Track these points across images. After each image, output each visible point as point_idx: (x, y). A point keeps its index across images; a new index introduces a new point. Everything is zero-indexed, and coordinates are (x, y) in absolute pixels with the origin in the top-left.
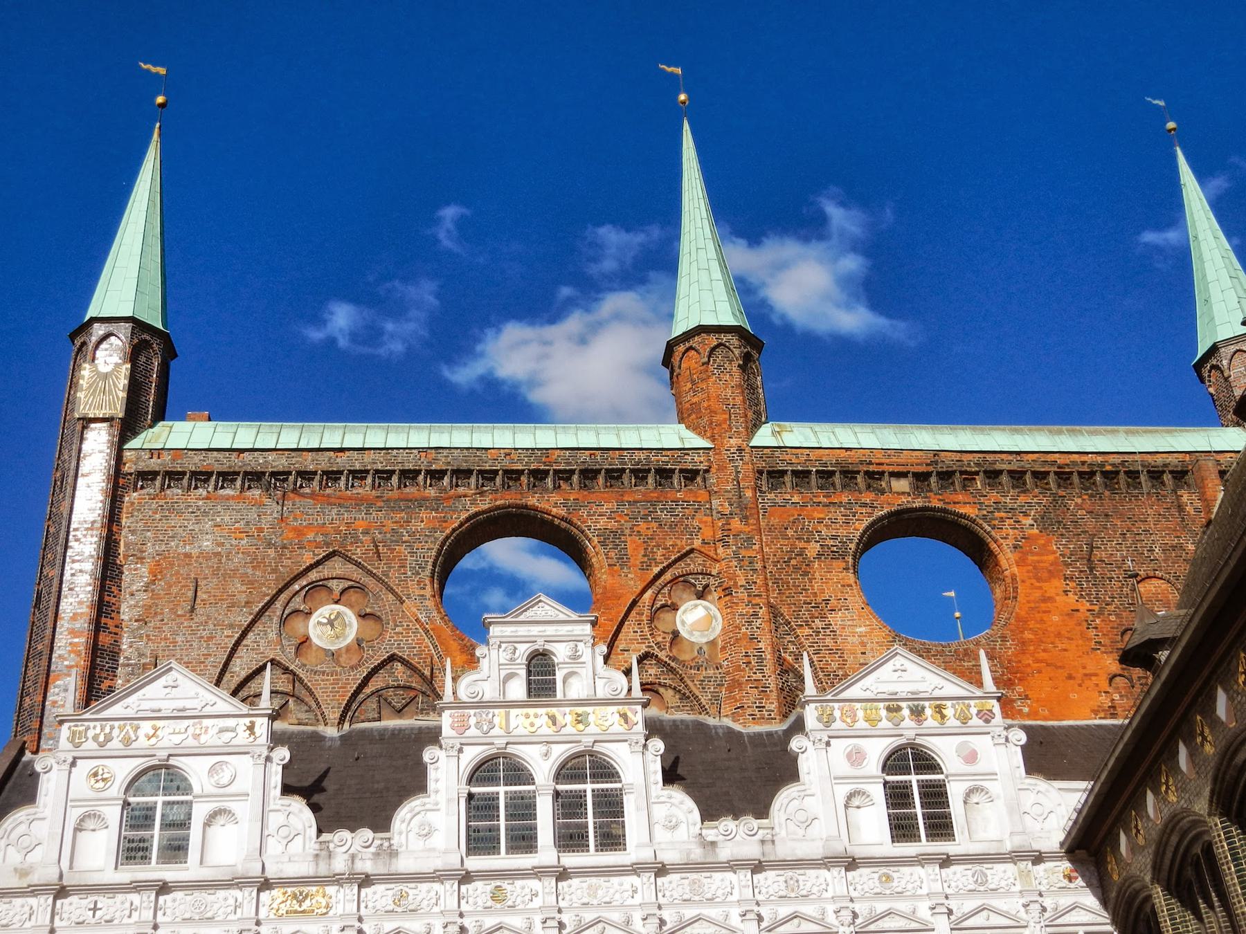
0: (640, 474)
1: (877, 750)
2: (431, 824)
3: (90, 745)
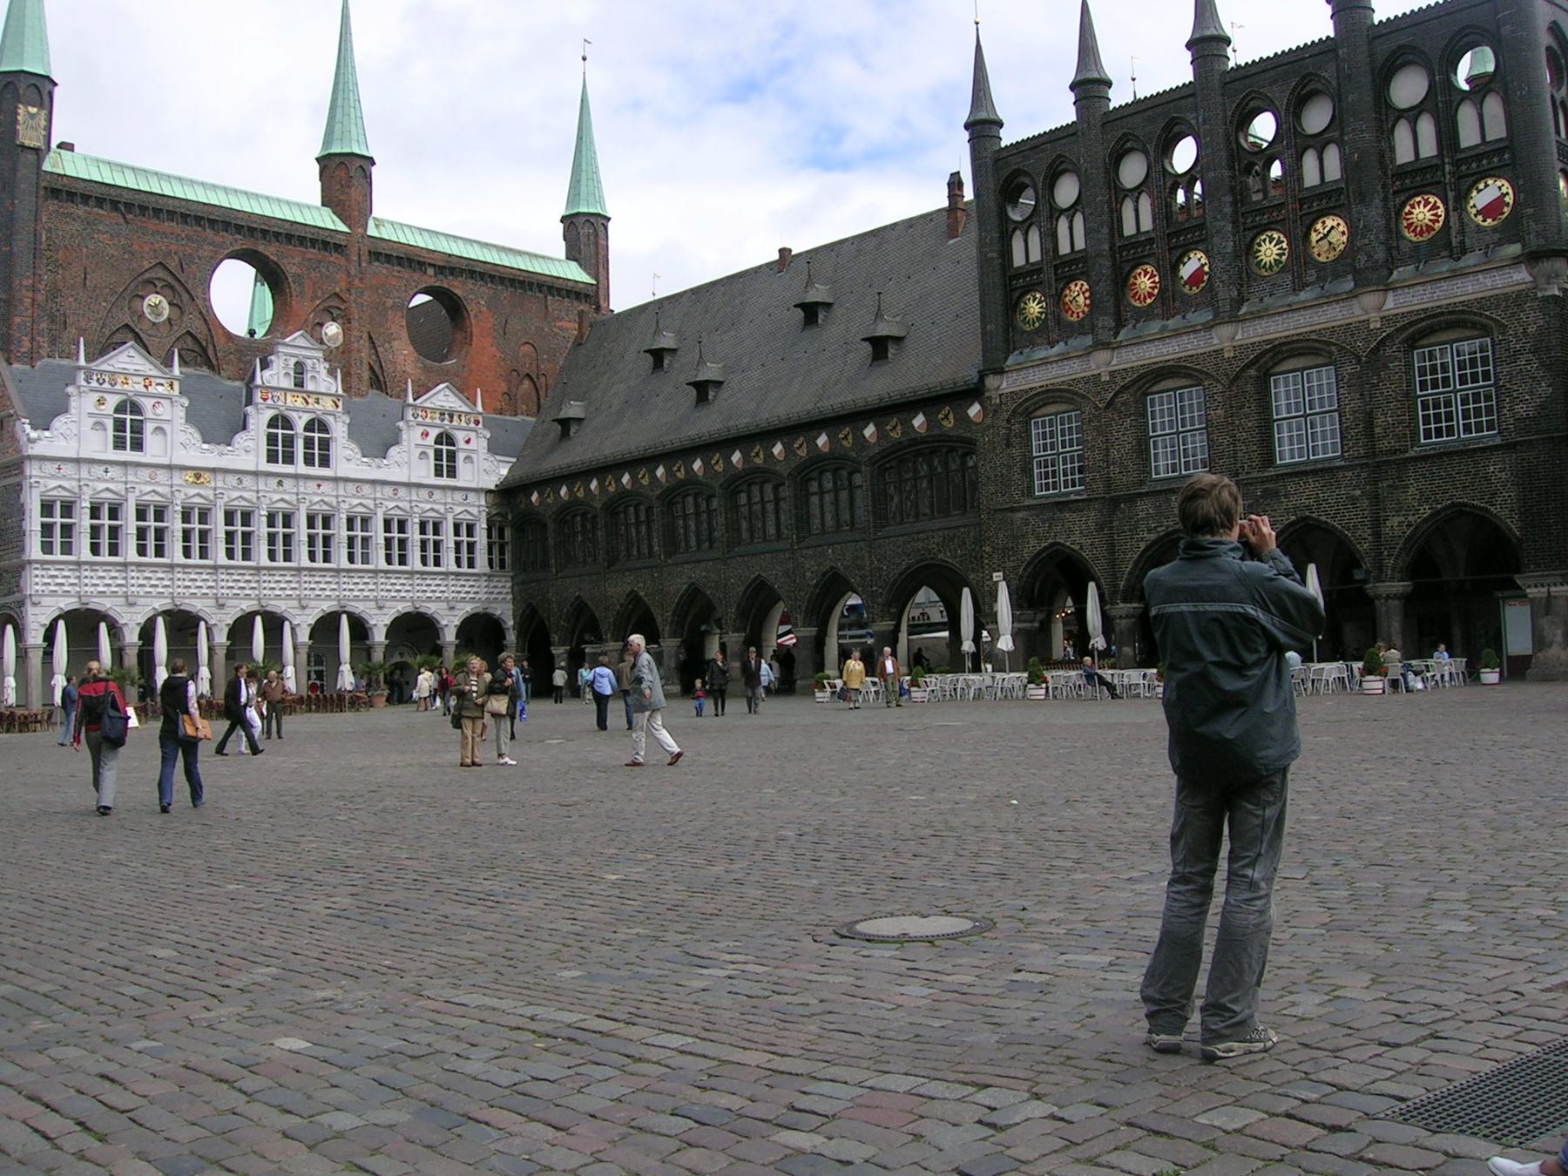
0: (314, 242)
1: (434, 433)
3: (94, 384)
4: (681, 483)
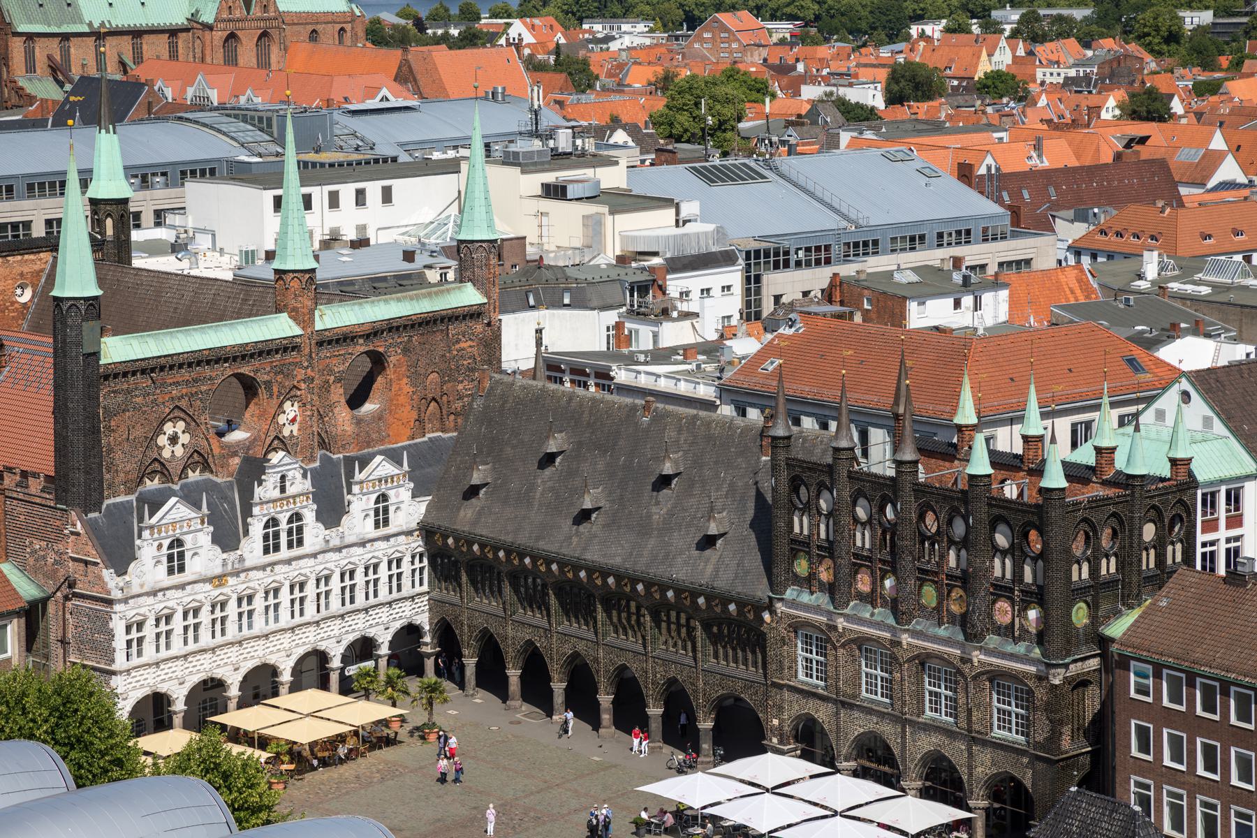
2: (252, 548)
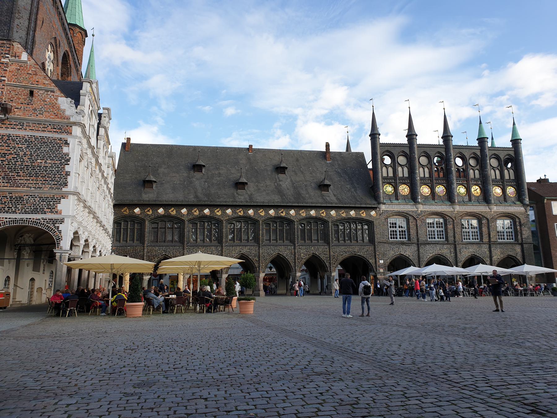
4: (240, 217)
